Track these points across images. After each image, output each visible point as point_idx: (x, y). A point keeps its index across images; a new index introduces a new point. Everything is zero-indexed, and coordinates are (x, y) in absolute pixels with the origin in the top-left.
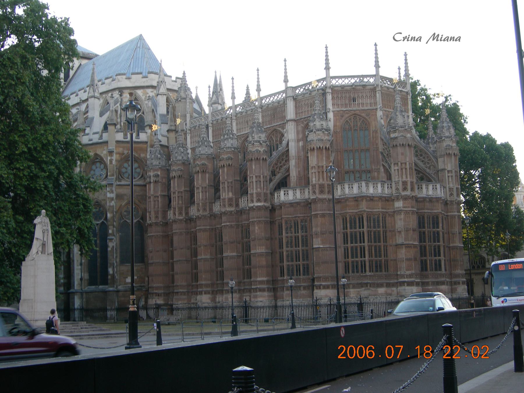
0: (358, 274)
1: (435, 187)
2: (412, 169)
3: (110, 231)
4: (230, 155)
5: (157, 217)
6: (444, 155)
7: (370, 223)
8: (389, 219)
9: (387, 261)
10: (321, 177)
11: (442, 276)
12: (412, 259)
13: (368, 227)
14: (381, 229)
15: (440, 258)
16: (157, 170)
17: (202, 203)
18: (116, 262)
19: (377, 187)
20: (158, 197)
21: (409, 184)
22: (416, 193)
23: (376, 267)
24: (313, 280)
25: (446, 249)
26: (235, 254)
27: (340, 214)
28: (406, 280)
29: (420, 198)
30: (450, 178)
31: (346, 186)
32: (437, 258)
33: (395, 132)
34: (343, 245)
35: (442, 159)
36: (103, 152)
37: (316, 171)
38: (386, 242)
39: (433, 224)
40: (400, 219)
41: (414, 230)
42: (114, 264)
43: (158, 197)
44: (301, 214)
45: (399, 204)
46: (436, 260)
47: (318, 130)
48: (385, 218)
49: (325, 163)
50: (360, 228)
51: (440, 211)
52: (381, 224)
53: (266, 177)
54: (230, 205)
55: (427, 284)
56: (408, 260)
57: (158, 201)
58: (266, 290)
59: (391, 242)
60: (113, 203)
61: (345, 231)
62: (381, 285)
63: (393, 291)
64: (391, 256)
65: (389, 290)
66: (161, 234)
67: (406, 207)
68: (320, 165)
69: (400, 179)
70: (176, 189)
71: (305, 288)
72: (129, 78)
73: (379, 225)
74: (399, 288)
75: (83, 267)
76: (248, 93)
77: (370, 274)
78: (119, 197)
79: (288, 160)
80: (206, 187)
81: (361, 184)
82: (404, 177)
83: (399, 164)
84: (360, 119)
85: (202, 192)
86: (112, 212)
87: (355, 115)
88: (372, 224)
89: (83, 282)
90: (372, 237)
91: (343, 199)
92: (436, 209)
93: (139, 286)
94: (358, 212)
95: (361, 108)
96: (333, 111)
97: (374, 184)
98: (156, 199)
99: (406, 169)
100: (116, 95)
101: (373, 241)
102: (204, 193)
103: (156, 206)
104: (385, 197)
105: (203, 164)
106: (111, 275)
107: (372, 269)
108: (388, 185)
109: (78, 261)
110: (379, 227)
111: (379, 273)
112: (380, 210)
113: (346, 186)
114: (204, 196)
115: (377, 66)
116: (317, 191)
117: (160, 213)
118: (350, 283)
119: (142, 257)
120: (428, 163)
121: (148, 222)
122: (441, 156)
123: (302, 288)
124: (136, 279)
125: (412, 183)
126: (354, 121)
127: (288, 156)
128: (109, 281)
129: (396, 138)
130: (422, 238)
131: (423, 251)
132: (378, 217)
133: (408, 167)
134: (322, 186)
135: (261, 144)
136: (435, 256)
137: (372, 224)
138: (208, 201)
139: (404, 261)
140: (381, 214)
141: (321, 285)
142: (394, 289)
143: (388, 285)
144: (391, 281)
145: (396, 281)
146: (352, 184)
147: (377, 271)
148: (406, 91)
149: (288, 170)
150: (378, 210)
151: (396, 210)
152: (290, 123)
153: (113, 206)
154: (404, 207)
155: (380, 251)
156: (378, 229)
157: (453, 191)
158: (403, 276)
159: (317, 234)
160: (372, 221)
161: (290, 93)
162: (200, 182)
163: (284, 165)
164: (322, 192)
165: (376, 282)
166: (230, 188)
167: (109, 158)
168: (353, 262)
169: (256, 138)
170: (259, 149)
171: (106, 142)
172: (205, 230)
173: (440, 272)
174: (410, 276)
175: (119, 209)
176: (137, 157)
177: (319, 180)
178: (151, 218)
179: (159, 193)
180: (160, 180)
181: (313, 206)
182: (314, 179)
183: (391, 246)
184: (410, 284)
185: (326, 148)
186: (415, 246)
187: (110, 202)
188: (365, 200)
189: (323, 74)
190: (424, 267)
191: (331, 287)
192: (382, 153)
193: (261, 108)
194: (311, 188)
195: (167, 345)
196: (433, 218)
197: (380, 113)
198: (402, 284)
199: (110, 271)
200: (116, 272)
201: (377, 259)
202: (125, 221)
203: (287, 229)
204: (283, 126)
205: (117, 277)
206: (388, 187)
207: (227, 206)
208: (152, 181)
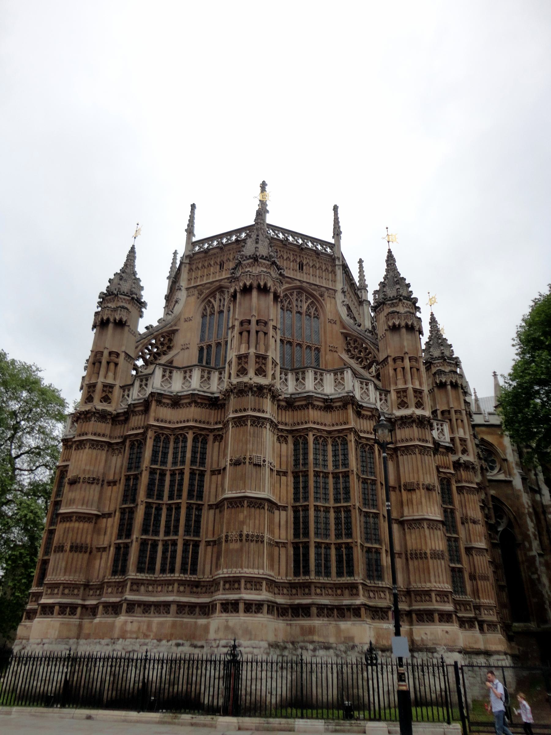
11: (352, 588)
21: (252, 360)
48: (205, 442)
52: (189, 455)
73: (184, 457)
96: (187, 289)
110: (183, 462)
126: (220, 300)
143: (182, 608)
185: (115, 320)
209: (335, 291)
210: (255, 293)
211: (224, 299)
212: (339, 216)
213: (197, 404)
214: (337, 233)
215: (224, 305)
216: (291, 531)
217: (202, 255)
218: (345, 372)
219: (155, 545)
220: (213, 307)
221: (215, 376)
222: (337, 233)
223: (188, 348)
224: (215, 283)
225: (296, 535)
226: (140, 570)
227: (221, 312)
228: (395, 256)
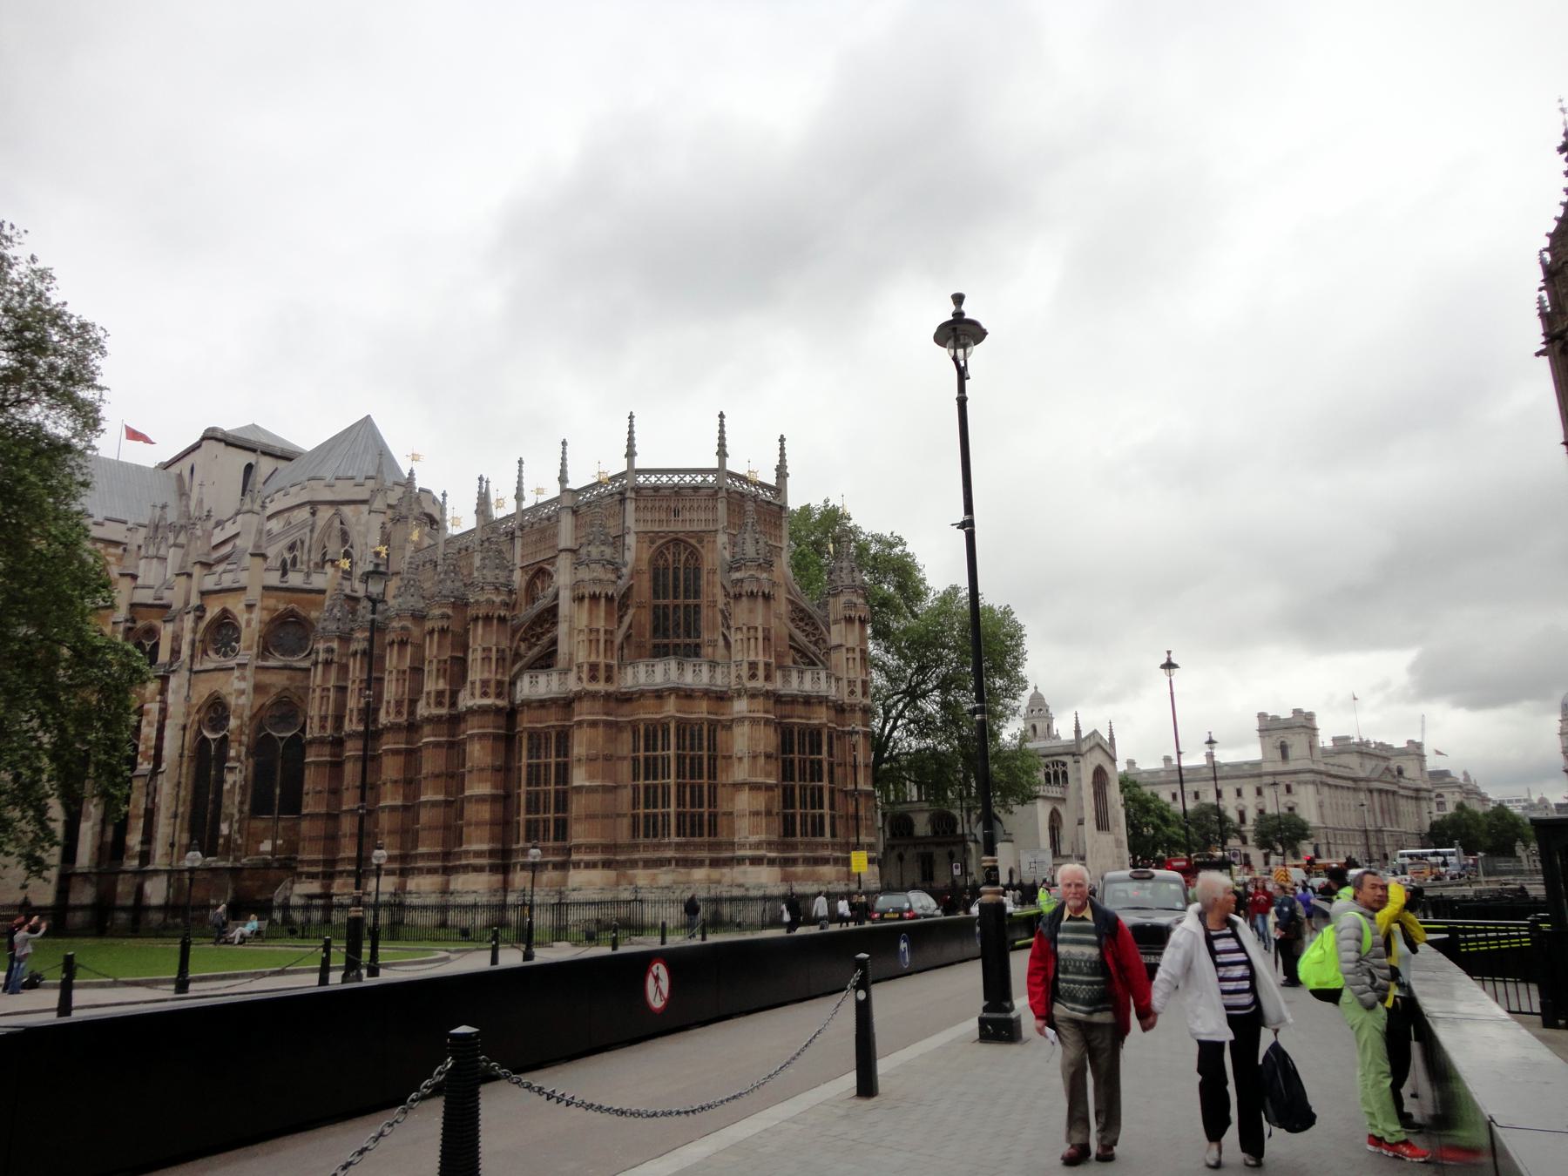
0: (655, 841)
2: (769, 640)
3: (232, 753)
4: (445, 610)
5: (323, 727)
7: (684, 739)
8: (721, 735)
9: (713, 817)
11: (824, 846)
13: (678, 749)
14: (705, 753)
16: (330, 640)
17: (397, 702)
18: (241, 812)
20: (328, 690)
22: (777, 684)
23: (693, 826)
24: (568, 851)
25: (838, 797)
26: (440, 797)
27: (629, 722)
29: (786, 695)
30: (851, 661)
31: (642, 668)
32: (817, 811)
33: (738, 569)
35: (838, 626)
36: (236, 606)
37: (585, 638)
38: (715, 778)
39: (811, 745)
40: (743, 735)
41: (768, 756)
42: (233, 815)
43: (328, 690)
44: (557, 720)
45: (740, 706)
46: (814, 816)
47: (597, 562)
48: (715, 731)
50: (663, 750)
51: (824, 720)
52: (705, 744)
53: (504, 650)
54: (439, 704)
55: (794, 862)
56: (756, 814)
57: (329, 697)
58: (488, 868)
59: (724, 778)
60: (243, 700)
62: (699, 863)
64: (723, 807)
65: (715, 873)
66: (329, 759)
68: (594, 626)
69: (745, 659)
70: (357, 673)
71: (556, 866)
72: (330, 486)
73: (701, 744)
75: (178, 820)
76: (483, 501)
77: (677, 840)
78: (259, 688)
79: (555, 624)
80: (404, 672)
82: (752, 653)
83: (745, 629)
84: (686, 549)
85: (397, 680)
86: (241, 717)
87: (677, 541)
88: (688, 742)
89: (176, 850)
90: (688, 768)
91: (635, 692)
93: (286, 859)
95: (688, 528)
96: (636, 533)
97: (695, 666)
98: (325, 693)
100: (305, 513)
101: (688, 775)
102: (401, 681)
103: (324, 708)
104: (716, 692)
105: (403, 628)
106: (224, 836)
107: (685, 830)
109: (168, 808)
110: (701, 748)
111: (697, 839)
112: (705, 715)
113: (642, 668)
114: (401, 686)
115: (722, 453)
116: (585, 676)
117: (330, 719)
119: (292, 803)
120: (814, 635)
121: (308, 736)
122: (836, 622)
123: (550, 867)
124: (281, 846)
125: (767, 665)
126: (674, 553)
127: (555, 615)
128: (220, 849)
129: (742, 581)
130: (787, 772)
131: (788, 800)
132: (701, 730)
133: (760, 635)
134: (594, 667)
135: (497, 589)
136: (813, 807)
137: (688, 742)
138: (406, 696)
141: (581, 860)
142: (726, 870)
143: (715, 863)
146: (653, 666)
147: (693, 835)
148: (779, 503)
149: (554, 642)
150: (700, 716)
151: (735, 716)
152: (563, 555)
153: (244, 705)
155: (701, 796)
157: (855, 686)
158: (742, 846)
159: (579, 760)
160: (688, 737)
161: (568, 502)
162: (395, 661)
163: (549, 632)
164: (593, 678)
166: (442, 671)
167: (246, 616)
168: (647, 816)
169: (490, 579)
170: (494, 598)
171: (243, 589)
172: (396, 752)
173: (819, 839)
174: (758, 845)
175: (257, 712)
176: (305, 618)
177: (590, 655)
178: (313, 732)
179: (332, 683)
180: (336, 659)
181: (576, 705)
182: (581, 654)
183: (724, 785)
184: (756, 861)
185: (607, 594)
186: (769, 788)
187: (237, 697)
188: (673, 697)
189: (621, 466)
190: (788, 828)
191: (600, 865)
192: (722, 611)
193: (522, 530)
194: (575, 669)
195: (207, 992)
196: (811, 734)
197: (722, 539)
198: (740, 861)
199: (224, 829)
200: (239, 831)
202: (269, 734)
203: (530, 750)
204: (552, 560)
205: (239, 841)
207: (432, 706)
208: (320, 659)
209: (781, 549)
211: (679, 554)
212: (786, 451)
213: (710, 698)
214: (781, 472)
215: (679, 561)
216: (781, 805)
217: (651, 492)
220: (666, 560)
221: (719, 670)
222: (781, 472)
225: (785, 807)
226: (678, 835)
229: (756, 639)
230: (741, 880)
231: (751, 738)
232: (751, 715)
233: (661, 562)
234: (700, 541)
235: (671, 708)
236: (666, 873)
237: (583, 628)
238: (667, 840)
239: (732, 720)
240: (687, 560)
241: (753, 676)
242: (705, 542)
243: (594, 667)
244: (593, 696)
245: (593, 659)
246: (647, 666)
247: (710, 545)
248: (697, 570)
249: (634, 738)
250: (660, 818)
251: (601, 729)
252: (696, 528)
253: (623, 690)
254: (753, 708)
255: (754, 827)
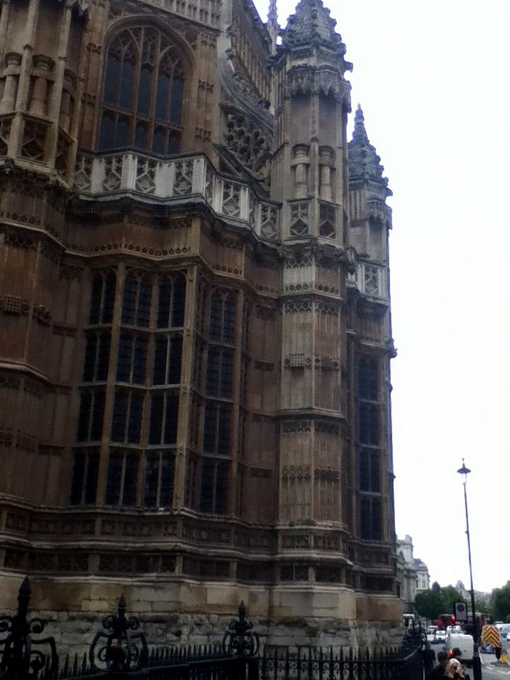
1: (371, 273)
6: (365, 220)
10: (39, 93)
12: (336, 474)
15: (378, 494)
19: (237, 197)
23: (206, 488)
27: (87, 261)
28: (314, 554)
31: (130, 165)
34: (78, 383)
35: (358, 230)
37: (23, 70)
40: (304, 327)
45: (302, 276)
49: (63, 52)
56: (325, 476)
61: (101, 324)
63: (253, 598)
67: (326, 289)
74: (279, 588)
81: (190, 165)
83: (315, 147)
84: (164, 46)
92: (372, 340)
94: (163, 262)
99: (333, 170)
108: (264, 210)
111: (215, 517)
112: (241, 277)
113: (130, 165)
118: (92, 549)
126: (145, 44)
132: (232, 302)
139: (308, 478)
140: (242, 292)
142: (259, 589)
143: (249, 572)
144: (252, 556)
145: (263, 556)
146: (152, 164)
150: (232, 275)
151: (286, 293)
154: (320, 288)
156: (228, 345)
158: (299, 539)
164: (32, 148)
165: (201, 550)
168: (116, 454)
174: (328, 540)
183: (257, 418)
184: (328, 573)
188: (196, 225)
192: (222, 149)
197: (224, 44)
198: (296, 570)
201: (210, 455)
206: (264, 218)
210: (316, 99)
211: (153, 48)
215: (152, 57)
218: (379, 270)
219: (134, 457)
220: (132, 48)
223: (92, 105)
224: (145, 9)
227: (148, 68)
228: (364, 115)
229: (333, 170)
230: (296, 611)
231: (320, 336)
232: (321, 293)
233: (125, 49)
234: (192, 38)
235: (191, 241)
236: (156, 586)
237: (18, 48)
238: (161, 511)
239: (279, 302)
240: (164, 60)
241: (327, 229)
242: (199, 41)
243: (35, 132)
244: (28, 182)
245: (37, 111)
246: (141, 162)
247: (206, 49)
248: (180, 78)
249: (96, 293)
250: (144, 463)
251: (37, 256)
252: (186, 14)
253: (82, 197)
254: (323, 282)
255: (322, 501)
